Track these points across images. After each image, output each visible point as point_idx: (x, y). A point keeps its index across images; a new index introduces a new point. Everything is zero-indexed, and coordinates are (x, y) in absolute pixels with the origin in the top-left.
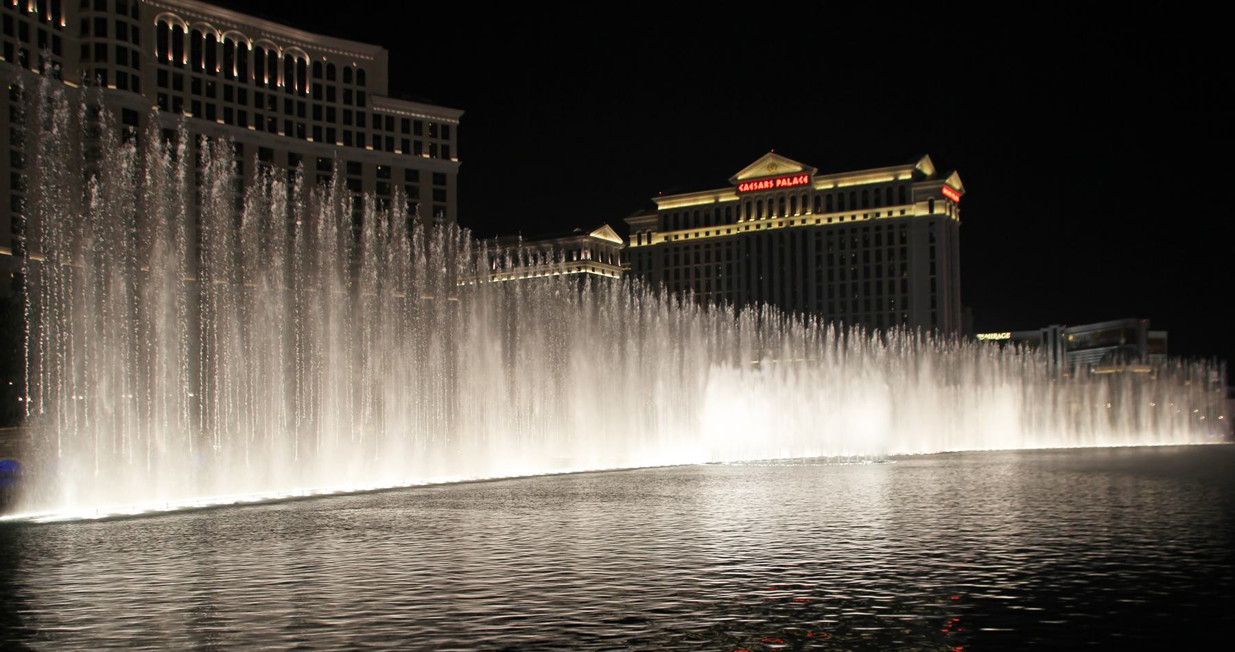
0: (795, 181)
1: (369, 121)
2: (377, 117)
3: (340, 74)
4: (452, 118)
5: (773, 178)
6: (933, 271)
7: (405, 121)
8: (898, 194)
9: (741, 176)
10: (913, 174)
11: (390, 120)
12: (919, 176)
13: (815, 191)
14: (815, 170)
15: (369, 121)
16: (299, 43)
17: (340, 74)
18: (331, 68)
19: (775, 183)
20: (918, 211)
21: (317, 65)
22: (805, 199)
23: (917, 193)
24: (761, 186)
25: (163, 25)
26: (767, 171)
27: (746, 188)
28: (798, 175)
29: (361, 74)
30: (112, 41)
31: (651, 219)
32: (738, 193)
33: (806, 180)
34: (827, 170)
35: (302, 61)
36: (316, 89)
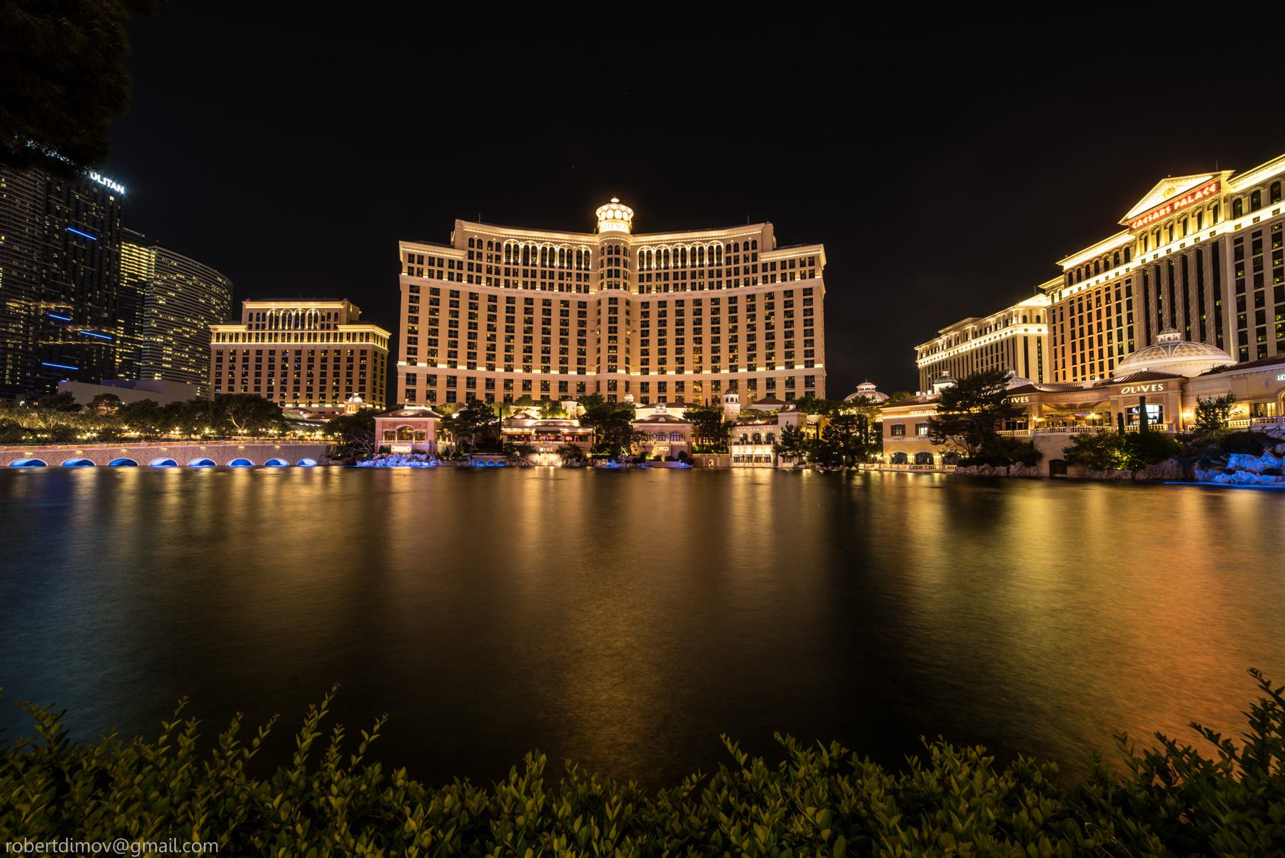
1: (760, 269)
2: (765, 265)
3: (741, 247)
4: (819, 251)
7: (783, 263)
11: (773, 264)
15: (760, 269)
16: (716, 237)
17: (741, 247)
18: (736, 245)
21: (728, 247)
25: (641, 254)
29: (754, 242)
30: (621, 268)
31: (1060, 280)
35: (719, 247)
36: (728, 261)
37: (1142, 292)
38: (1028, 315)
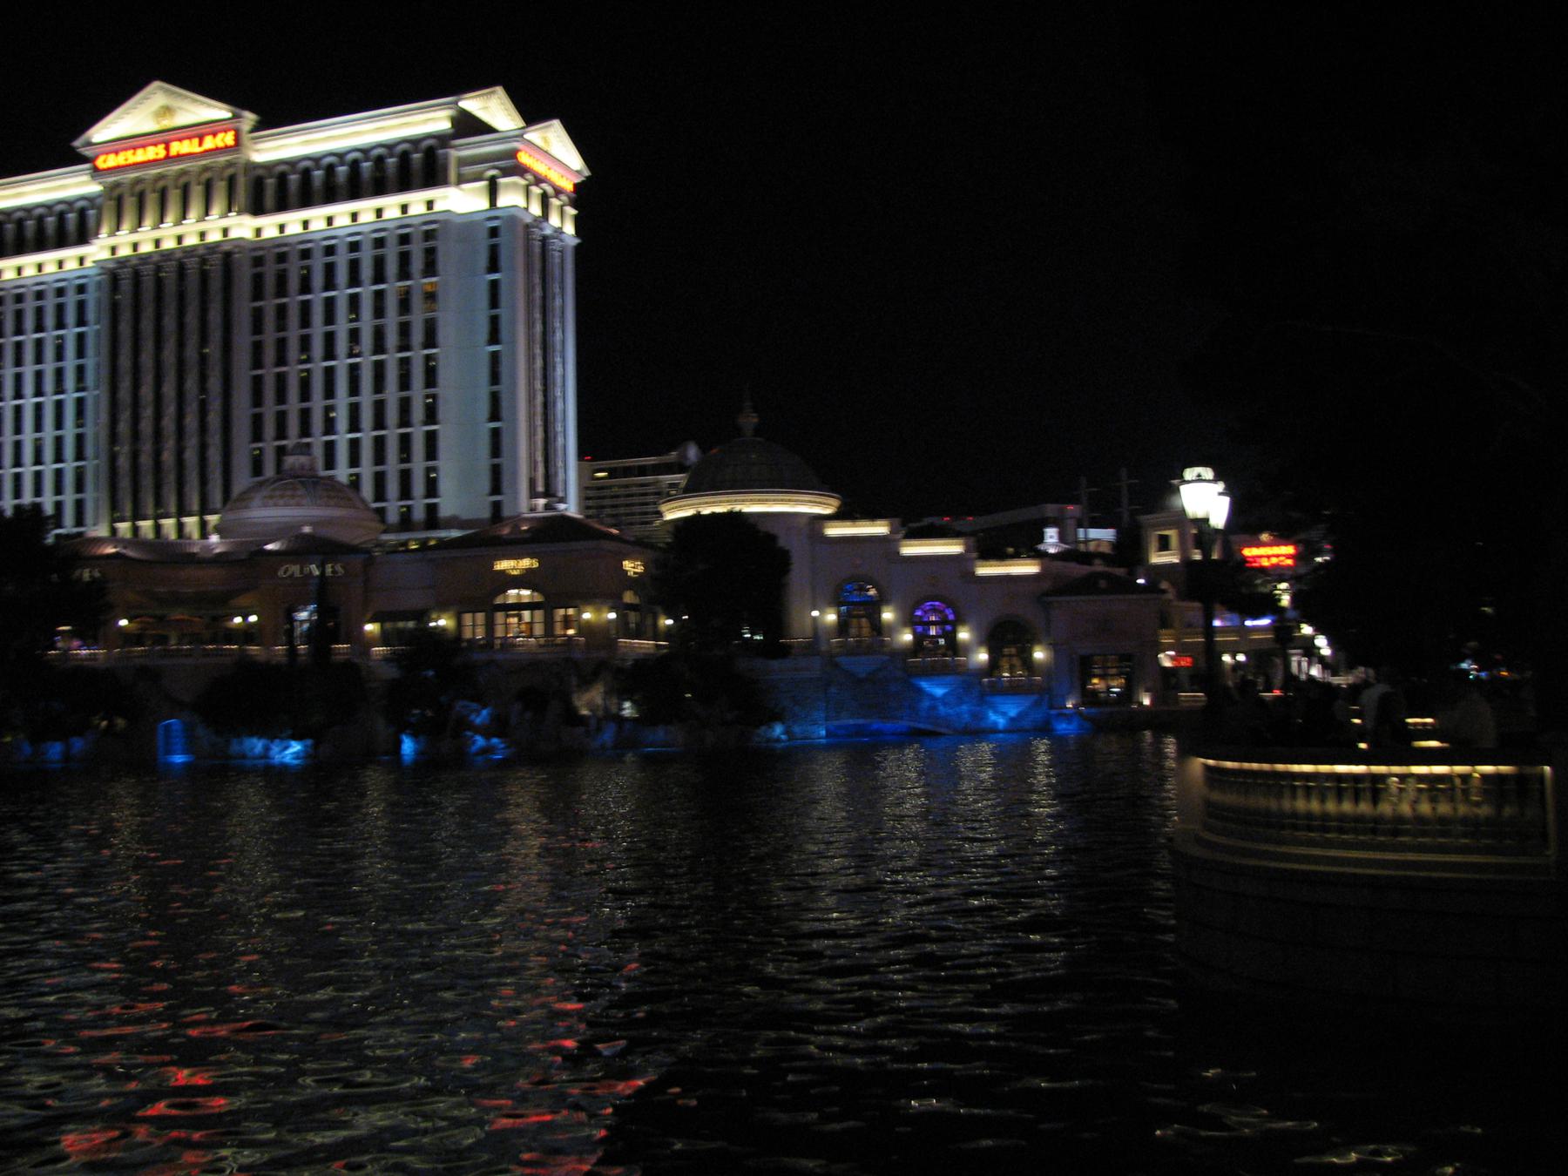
0: (209, 143)
5: (164, 137)
8: (420, 166)
9: (102, 132)
10: (454, 120)
12: (469, 126)
14: (250, 118)
19: (167, 149)
20: (460, 200)
22: (231, 182)
23: (463, 162)
24: (141, 156)
26: (150, 122)
27: (111, 161)
28: (213, 127)
32: (96, 172)
33: (229, 139)
34: (274, 117)
37: (106, 322)
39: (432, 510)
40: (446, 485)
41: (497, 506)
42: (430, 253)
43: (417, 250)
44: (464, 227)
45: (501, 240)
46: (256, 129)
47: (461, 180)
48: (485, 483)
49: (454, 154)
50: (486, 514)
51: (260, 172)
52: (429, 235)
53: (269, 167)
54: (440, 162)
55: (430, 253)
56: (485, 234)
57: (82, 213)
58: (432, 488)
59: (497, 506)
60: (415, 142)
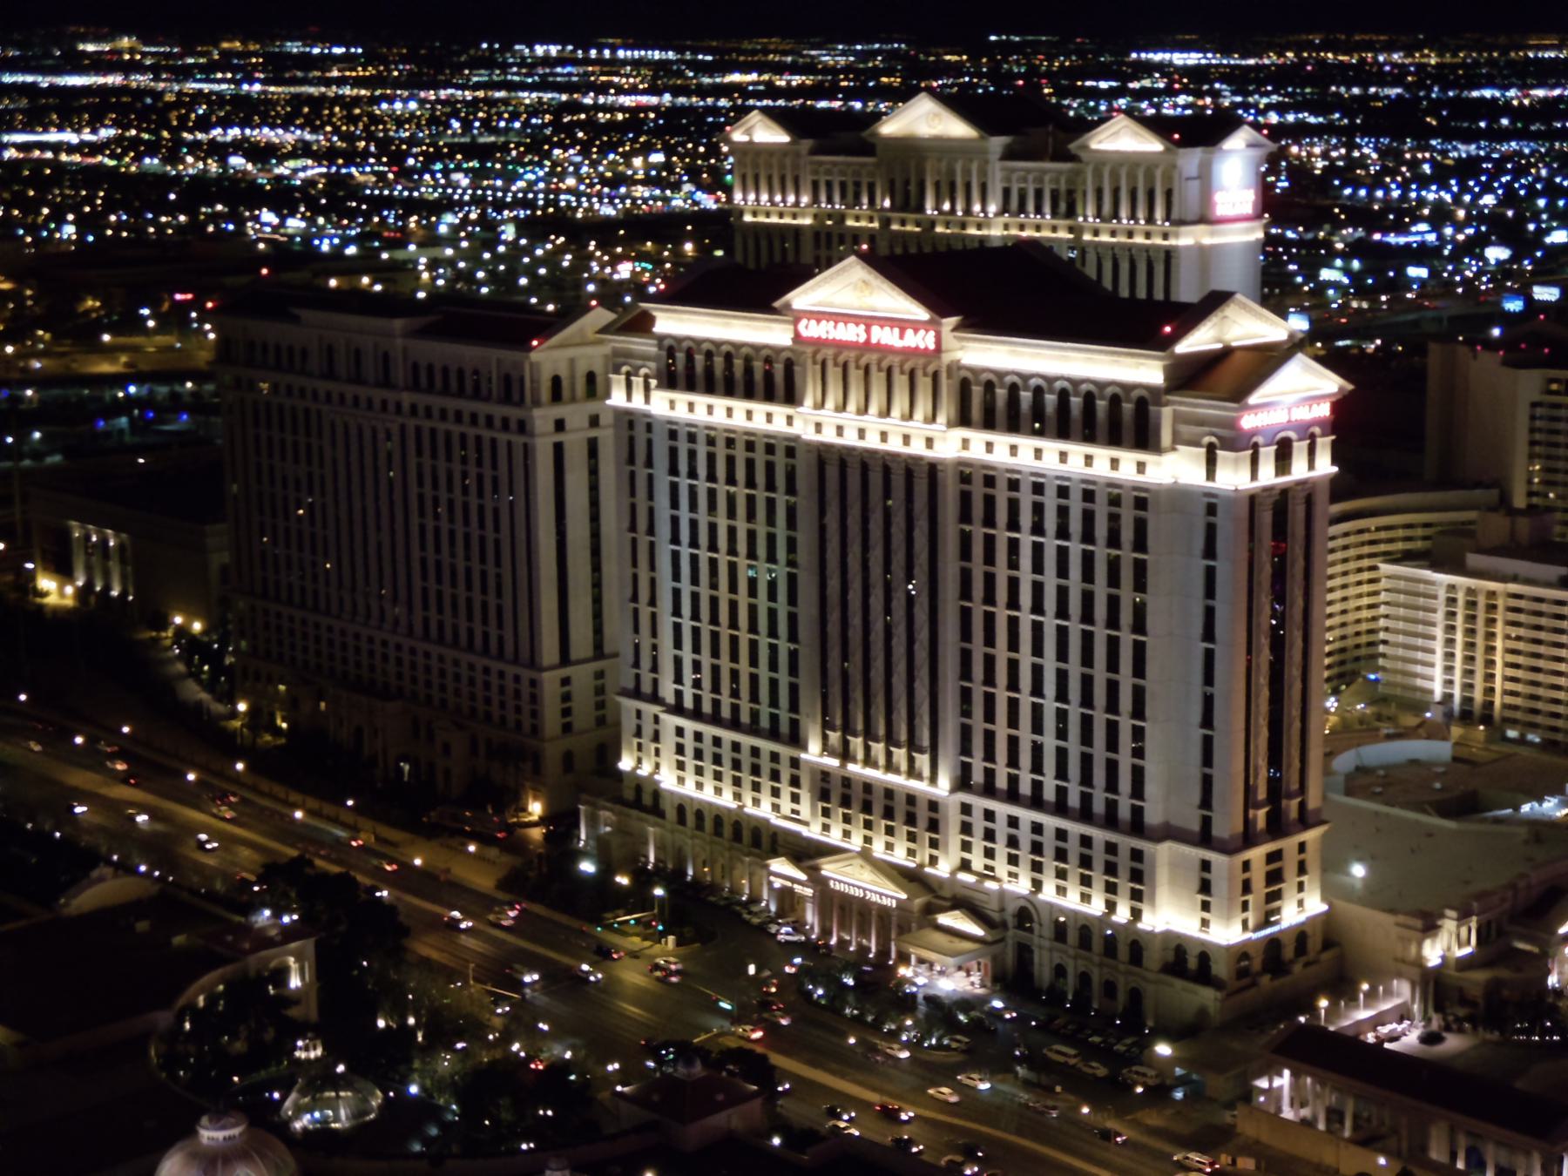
6: (1209, 634)
9: (801, 298)
13: (955, 367)
20: (1175, 468)
38: (564, 374)
39: (1137, 812)
40: (1150, 788)
41: (1206, 822)
42: (1141, 527)
43: (1127, 515)
44: (1178, 496)
45: (1220, 520)
46: (955, 330)
47: (1177, 440)
48: (1196, 796)
49: (1167, 413)
50: (1195, 826)
51: (969, 375)
52: (1141, 503)
53: (976, 371)
54: (1152, 421)
55: (1141, 527)
56: (1202, 510)
57: (789, 366)
58: (1138, 791)
59: (1206, 822)
60: (1128, 388)
